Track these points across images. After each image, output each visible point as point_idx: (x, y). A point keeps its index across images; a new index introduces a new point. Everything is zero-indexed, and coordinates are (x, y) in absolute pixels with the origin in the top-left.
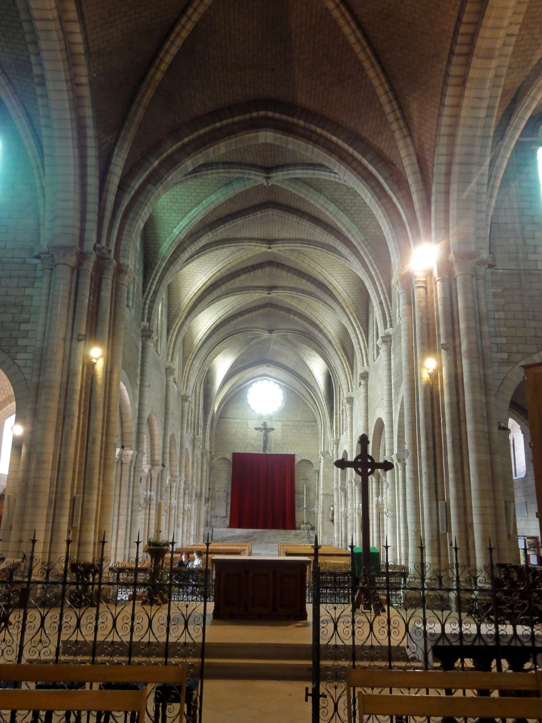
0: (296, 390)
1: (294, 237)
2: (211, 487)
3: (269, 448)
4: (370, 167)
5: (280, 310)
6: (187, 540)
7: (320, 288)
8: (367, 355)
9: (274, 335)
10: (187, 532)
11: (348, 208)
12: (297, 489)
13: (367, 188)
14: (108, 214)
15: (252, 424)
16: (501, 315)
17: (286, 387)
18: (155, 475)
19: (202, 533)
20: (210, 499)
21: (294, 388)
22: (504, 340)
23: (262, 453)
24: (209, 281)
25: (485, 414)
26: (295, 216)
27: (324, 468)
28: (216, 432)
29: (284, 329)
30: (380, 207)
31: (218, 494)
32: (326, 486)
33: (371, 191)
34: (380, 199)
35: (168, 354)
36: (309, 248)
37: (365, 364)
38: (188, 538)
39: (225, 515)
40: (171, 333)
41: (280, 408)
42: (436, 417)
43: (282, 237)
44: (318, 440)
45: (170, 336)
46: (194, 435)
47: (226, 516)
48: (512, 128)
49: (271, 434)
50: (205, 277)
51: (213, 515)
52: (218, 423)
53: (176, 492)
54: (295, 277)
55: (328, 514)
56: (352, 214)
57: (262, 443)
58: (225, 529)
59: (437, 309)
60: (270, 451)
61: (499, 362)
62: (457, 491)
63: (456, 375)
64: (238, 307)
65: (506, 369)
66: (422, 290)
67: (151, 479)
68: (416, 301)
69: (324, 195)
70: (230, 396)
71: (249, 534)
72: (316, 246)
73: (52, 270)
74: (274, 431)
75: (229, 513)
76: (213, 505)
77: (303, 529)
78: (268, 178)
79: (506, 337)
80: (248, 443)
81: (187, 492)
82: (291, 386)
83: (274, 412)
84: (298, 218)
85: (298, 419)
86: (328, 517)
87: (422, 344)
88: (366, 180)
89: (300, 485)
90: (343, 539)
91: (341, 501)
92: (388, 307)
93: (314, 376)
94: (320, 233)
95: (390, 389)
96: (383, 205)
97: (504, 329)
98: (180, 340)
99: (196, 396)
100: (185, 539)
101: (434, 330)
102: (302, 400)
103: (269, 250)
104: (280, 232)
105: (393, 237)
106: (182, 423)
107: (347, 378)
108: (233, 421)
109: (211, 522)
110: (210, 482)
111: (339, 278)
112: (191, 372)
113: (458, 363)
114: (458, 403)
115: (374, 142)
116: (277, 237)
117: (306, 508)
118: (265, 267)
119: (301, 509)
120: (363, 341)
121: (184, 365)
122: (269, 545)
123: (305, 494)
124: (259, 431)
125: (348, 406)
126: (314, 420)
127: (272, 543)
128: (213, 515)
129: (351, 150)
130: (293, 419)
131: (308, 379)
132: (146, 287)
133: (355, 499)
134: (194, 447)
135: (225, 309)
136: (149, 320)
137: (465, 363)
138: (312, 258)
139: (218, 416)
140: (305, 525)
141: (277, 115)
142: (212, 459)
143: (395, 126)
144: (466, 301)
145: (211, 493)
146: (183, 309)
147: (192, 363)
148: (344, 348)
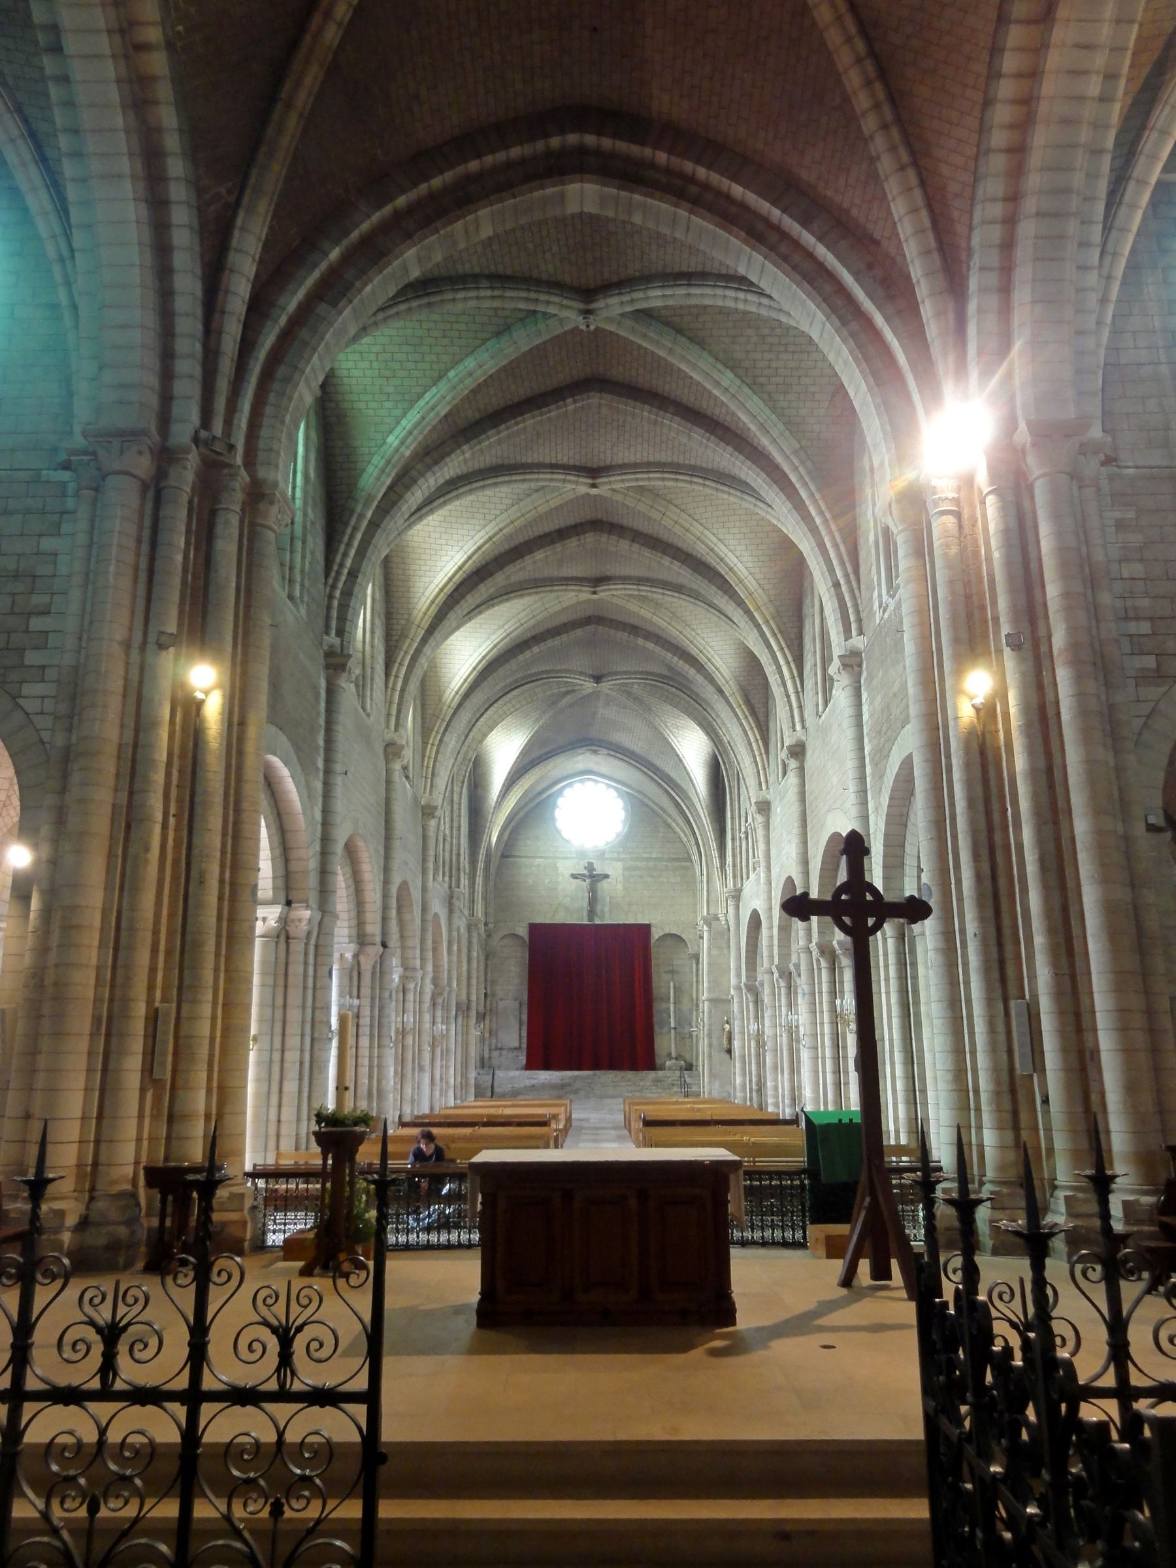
1: (645, 460)
3: (599, 913)
4: (821, 251)
5: (617, 629)
6: (441, 1095)
7: (700, 574)
8: (800, 707)
9: (605, 686)
10: (441, 1079)
11: (761, 380)
12: (655, 992)
13: (813, 301)
14: (226, 365)
15: (566, 868)
16: (1138, 569)
17: (628, 793)
18: (367, 964)
19: (472, 1081)
21: (644, 795)
22: (1145, 627)
23: (586, 922)
24: (470, 562)
25: (1116, 795)
26: (647, 407)
27: (709, 949)
29: (625, 673)
30: (844, 341)
31: (501, 1004)
32: (715, 984)
33: (824, 305)
34: (844, 323)
35: (389, 715)
36: (677, 480)
37: (798, 727)
38: (444, 1093)
39: (516, 1044)
40: (394, 672)
41: (618, 835)
42: (995, 806)
43: (620, 462)
44: (695, 895)
45: (392, 679)
46: (450, 887)
48: (1154, 135)
49: (604, 885)
50: (461, 553)
52: (499, 868)
53: (415, 1001)
54: (647, 552)
55: (720, 1038)
56: (769, 394)
57: (585, 904)
58: (518, 1073)
59: (989, 559)
60: (602, 917)
61: (1135, 678)
62: (1057, 975)
63: (1042, 709)
64: (531, 623)
65: (1151, 692)
66: (950, 520)
67: (359, 973)
68: (936, 545)
69: (710, 352)
70: (522, 814)
71: (567, 1081)
72: (692, 475)
73: (96, 489)
75: (525, 1040)
76: (494, 1027)
77: (670, 1069)
78: (587, 313)
79: (1151, 619)
81: (440, 1001)
82: (640, 792)
84: (654, 410)
85: (654, 855)
86: (721, 1044)
87: (956, 641)
88: (811, 282)
89: (662, 983)
90: (754, 1087)
91: (748, 1011)
92: (852, 591)
93: (685, 767)
94: (701, 443)
95: (862, 766)
96: (853, 335)
97: (1145, 603)
98: (413, 686)
99: (452, 811)
100: (437, 1094)
101: (983, 608)
102: (661, 817)
103: (594, 491)
104: (615, 449)
105: (877, 407)
106: (424, 860)
107: (756, 762)
110: (486, 980)
111: (739, 548)
112: (440, 757)
113: (1047, 680)
114: (1050, 770)
115: (829, 193)
116: (608, 462)
118: (584, 533)
119: (665, 1030)
120: (793, 677)
121: (425, 743)
125: (760, 819)
127: (612, 1097)
129: (776, 214)
131: (673, 775)
132: (333, 562)
133: (780, 1006)
134: (451, 912)
135: (506, 627)
136: (340, 633)
137: (1063, 677)
138: (683, 507)
139: (499, 854)
140: (674, 1061)
141: (607, 143)
142: (489, 936)
143: (879, 143)
144: (1059, 534)
146: (416, 622)
147: (441, 741)
148: (748, 702)
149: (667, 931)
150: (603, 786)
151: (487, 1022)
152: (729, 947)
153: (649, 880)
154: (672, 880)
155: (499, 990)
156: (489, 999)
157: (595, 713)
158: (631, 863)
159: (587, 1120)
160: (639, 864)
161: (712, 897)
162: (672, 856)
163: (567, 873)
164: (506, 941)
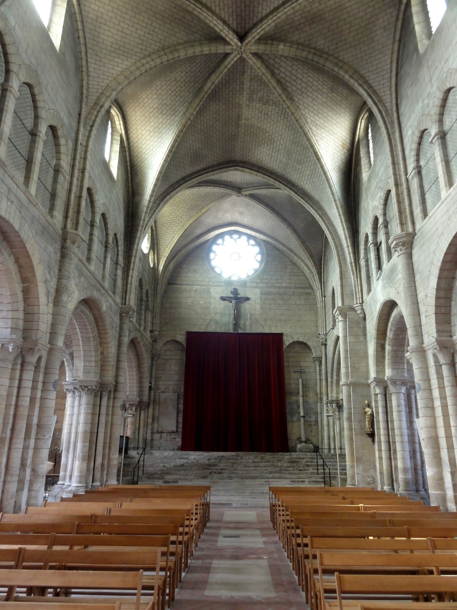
0: (281, 243)
2: (153, 386)
3: (242, 326)
10: (23, 465)
12: (287, 387)
17: (264, 241)
20: (152, 403)
21: (277, 240)
23: (231, 331)
28: (162, 304)
31: (163, 396)
39: (174, 429)
41: (256, 271)
44: (316, 314)
47: (177, 431)
49: (246, 306)
51: (155, 430)
52: (166, 291)
55: (362, 421)
57: (231, 319)
58: (171, 453)
60: (245, 329)
70: (183, 252)
71: (212, 461)
74: (250, 302)
75: (180, 425)
76: (157, 414)
77: (301, 451)
80: (211, 320)
83: (248, 276)
85: (284, 285)
86: (363, 428)
108: (188, 287)
109: (152, 440)
110: (151, 377)
117: (304, 417)
119: (295, 418)
122: (248, 482)
123: (301, 394)
124: (227, 302)
126: (308, 285)
127: (253, 478)
128: (155, 430)
130: (278, 285)
139: (165, 280)
140: (303, 444)
142: (155, 341)
145: (152, 394)
149: (296, 340)
150: (244, 238)
151: (151, 410)
152: (365, 335)
153: (280, 302)
154: (298, 303)
155: (162, 385)
156: (152, 392)
157: (239, 118)
158: (268, 290)
159: (229, 505)
160: (272, 290)
161: (347, 291)
162: (298, 286)
163: (218, 296)
164: (169, 346)
